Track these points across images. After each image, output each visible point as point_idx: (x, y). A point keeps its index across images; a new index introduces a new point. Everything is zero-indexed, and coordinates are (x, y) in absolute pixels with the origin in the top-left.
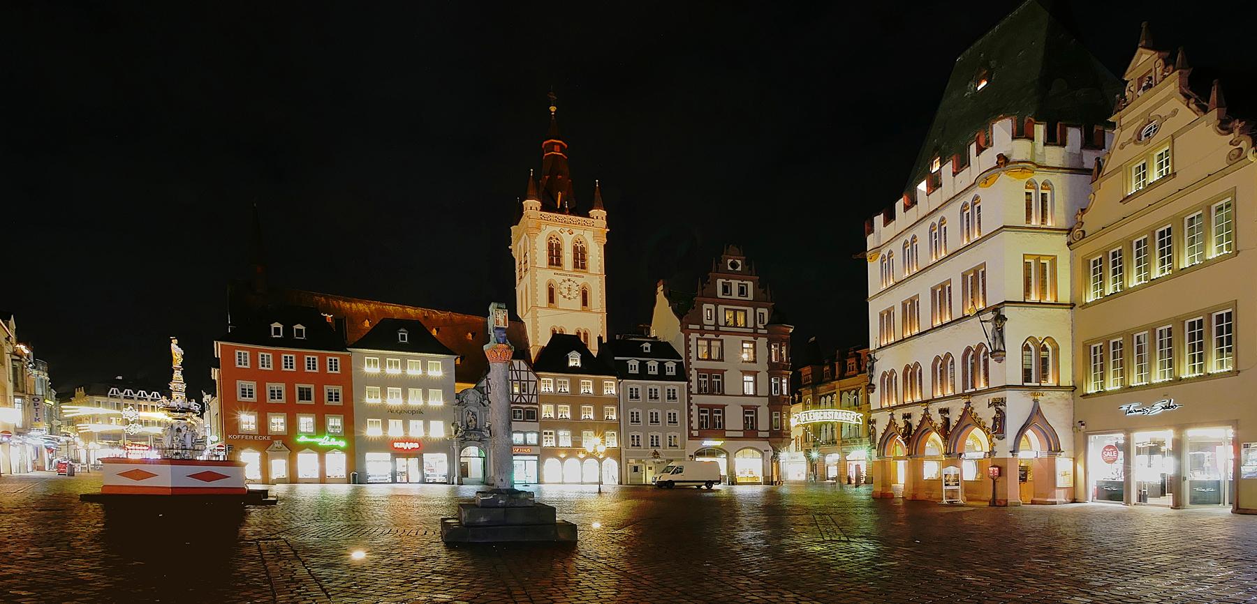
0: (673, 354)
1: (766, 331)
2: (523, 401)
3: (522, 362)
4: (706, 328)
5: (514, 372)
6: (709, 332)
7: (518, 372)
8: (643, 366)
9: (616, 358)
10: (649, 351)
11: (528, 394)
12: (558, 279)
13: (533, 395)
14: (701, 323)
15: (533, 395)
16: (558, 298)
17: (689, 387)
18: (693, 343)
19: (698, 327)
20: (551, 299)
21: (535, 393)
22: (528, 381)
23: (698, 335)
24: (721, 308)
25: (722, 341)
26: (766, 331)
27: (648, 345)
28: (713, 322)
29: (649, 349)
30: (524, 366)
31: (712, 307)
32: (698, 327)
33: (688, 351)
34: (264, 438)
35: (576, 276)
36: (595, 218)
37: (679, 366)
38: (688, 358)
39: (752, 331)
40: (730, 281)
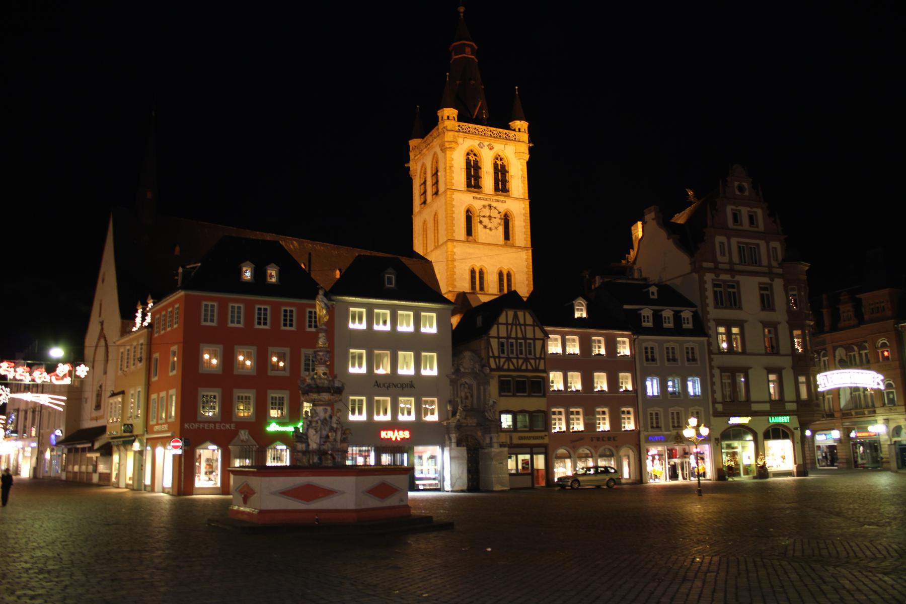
0: (687, 303)
1: (780, 271)
2: (530, 367)
3: (527, 315)
4: (721, 266)
5: (518, 327)
6: (726, 271)
7: (523, 327)
8: (657, 316)
9: (626, 307)
10: (655, 297)
11: (535, 359)
12: (477, 205)
13: (540, 358)
14: (716, 262)
15: (540, 358)
16: (478, 229)
18: (709, 286)
19: (711, 265)
20: (469, 232)
21: (543, 356)
22: (534, 339)
24: (734, 241)
25: (738, 282)
26: (780, 271)
27: (653, 289)
28: (726, 259)
29: (656, 293)
30: (529, 320)
32: (711, 265)
33: (703, 298)
34: (228, 426)
35: (498, 201)
36: (517, 130)
37: (695, 316)
38: (704, 305)
39: (766, 270)
40: (739, 208)
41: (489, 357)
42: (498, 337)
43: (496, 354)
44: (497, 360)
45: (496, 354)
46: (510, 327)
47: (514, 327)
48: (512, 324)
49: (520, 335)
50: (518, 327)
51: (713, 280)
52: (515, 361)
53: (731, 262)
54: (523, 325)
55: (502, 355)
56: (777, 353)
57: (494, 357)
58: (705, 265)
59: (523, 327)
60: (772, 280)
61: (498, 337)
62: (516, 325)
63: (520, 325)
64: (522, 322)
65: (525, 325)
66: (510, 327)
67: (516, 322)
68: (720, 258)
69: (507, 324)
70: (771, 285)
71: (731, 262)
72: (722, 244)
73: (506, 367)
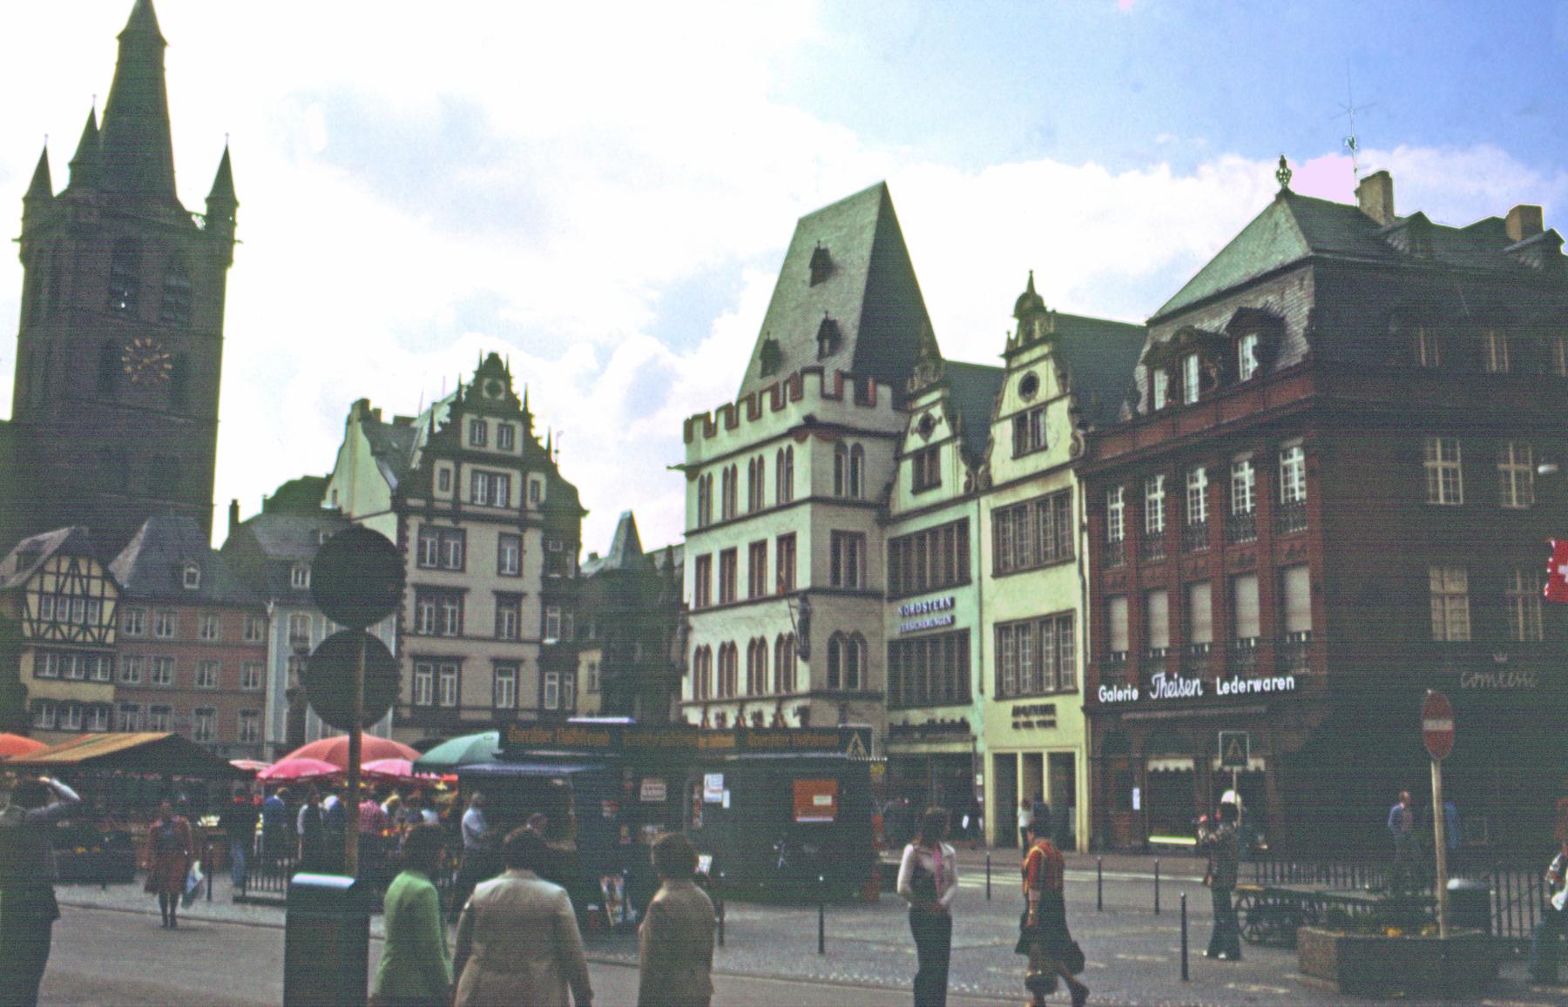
1: (539, 517)
4: (438, 505)
6: (443, 514)
7: (85, 581)
11: (100, 626)
13: (108, 627)
14: (430, 499)
15: (108, 627)
17: (401, 620)
21: (113, 624)
22: (102, 599)
23: (423, 520)
24: (466, 469)
25: (464, 532)
26: (539, 517)
28: (449, 495)
31: (449, 465)
39: (515, 514)
40: (486, 418)
41: (21, 620)
42: (41, 593)
43: (34, 615)
44: (35, 626)
45: (34, 615)
46: (61, 579)
47: (69, 580)
48: (66, 575)
49: (78, 591)
50: (77, 580)
51: (421, 525)
52: (65, 629)
53: (456, 501)
54: (85, 577)
55: (43, 618)
56: (519, 640)
57: (30, 621)
58: (412, 502)
59: (85, 581)
60: (524, 531)
61: (41, 593)
62: (73, 577)
63: (81, 577)
64: (84, 571)
65: (89, 577)
66: (61, 579)
67: (74, 572)
68: (437, 493)
69: (58, 574)
70: (520, 539)
71: (456, 501)
72: (445, 472)
73: (49, 635)
